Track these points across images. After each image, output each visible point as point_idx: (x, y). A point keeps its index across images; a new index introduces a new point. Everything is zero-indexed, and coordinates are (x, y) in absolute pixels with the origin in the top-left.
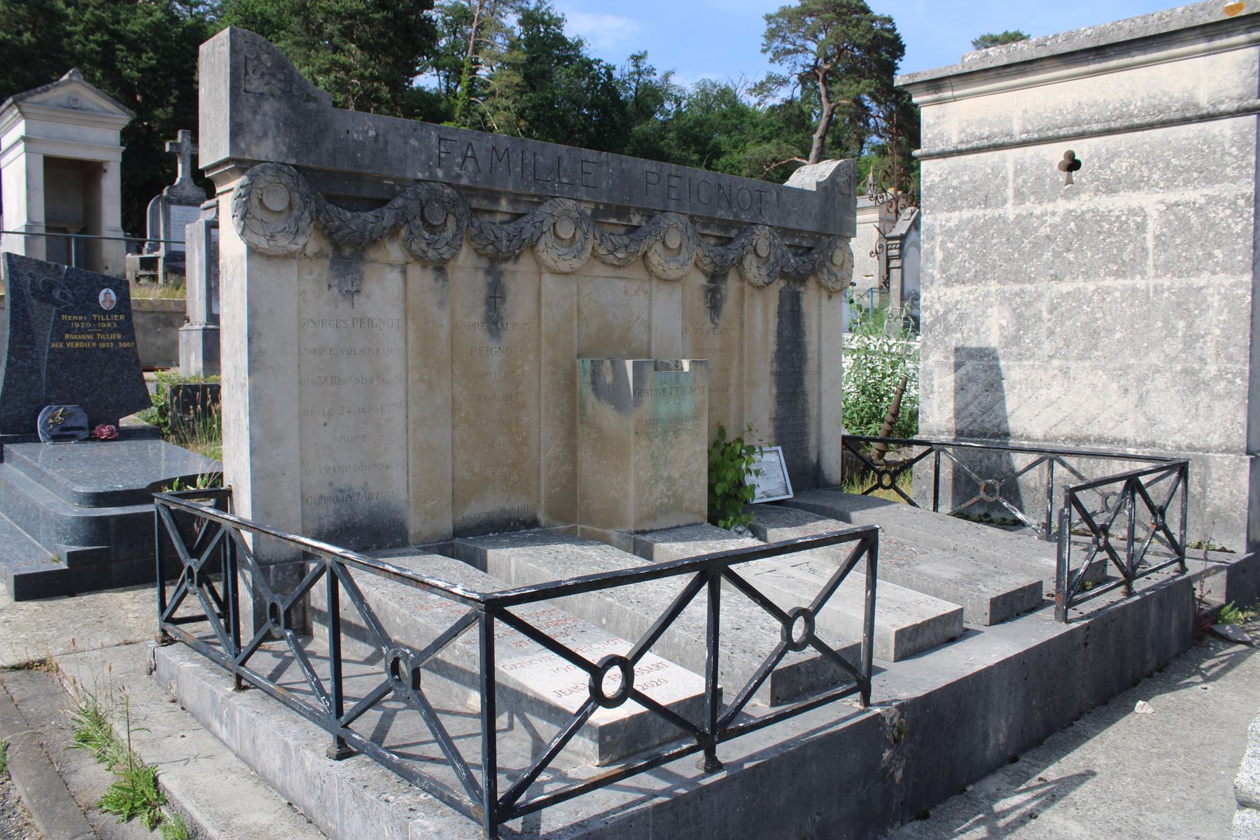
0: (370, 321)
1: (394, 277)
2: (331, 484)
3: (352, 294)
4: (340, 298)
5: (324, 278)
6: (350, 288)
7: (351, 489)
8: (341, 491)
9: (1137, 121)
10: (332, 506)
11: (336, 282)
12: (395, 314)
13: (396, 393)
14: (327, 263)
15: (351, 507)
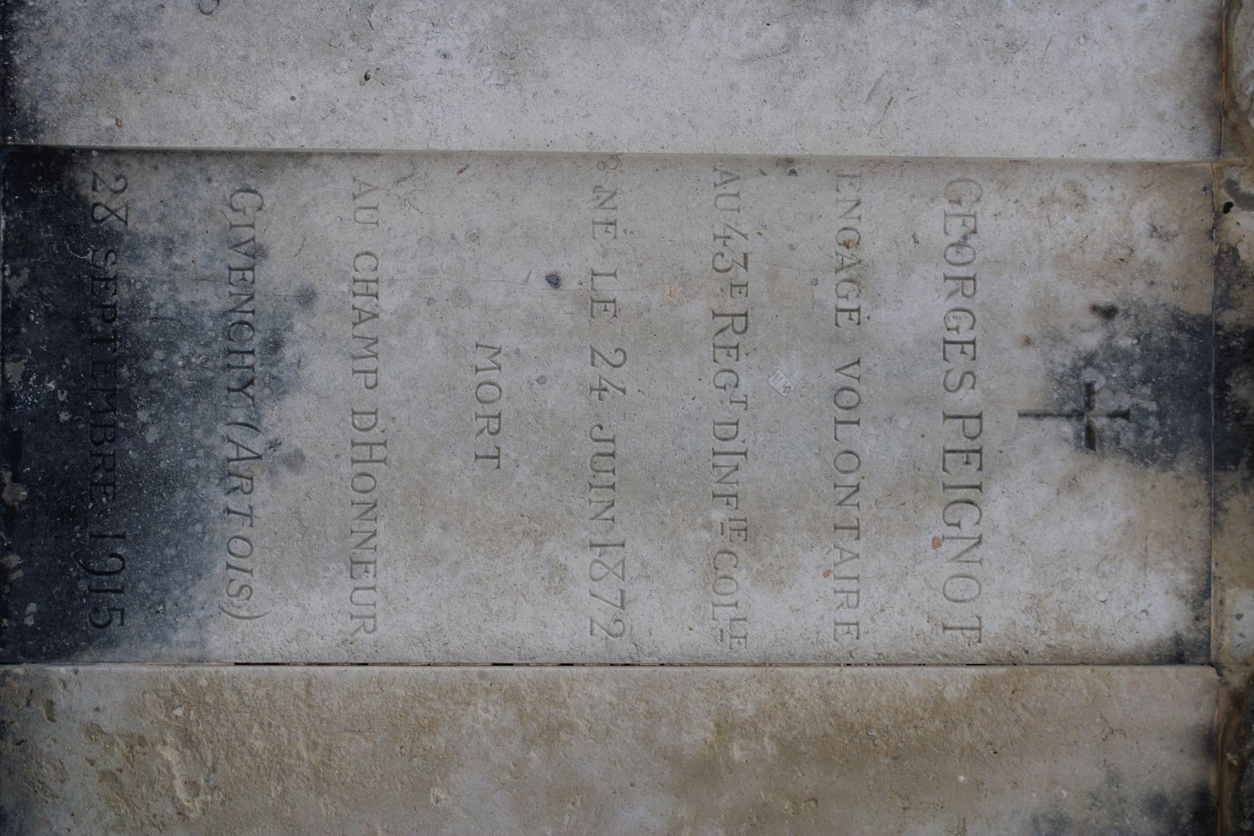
0: (972, 496)
1: (1157, 611)
2: (307, 298)
3: (1078, 409)
4: (1063, 358)
5: (1138, 287)
6: (1106, 401)
7: (279, 388)
8: (275, 346)
9: (463, 661)
10: (214, 299)
11: (1125, 342)
12: (1002, 609)
13: (670, 619)
14: (1199, 301)
15: (202, 387)
